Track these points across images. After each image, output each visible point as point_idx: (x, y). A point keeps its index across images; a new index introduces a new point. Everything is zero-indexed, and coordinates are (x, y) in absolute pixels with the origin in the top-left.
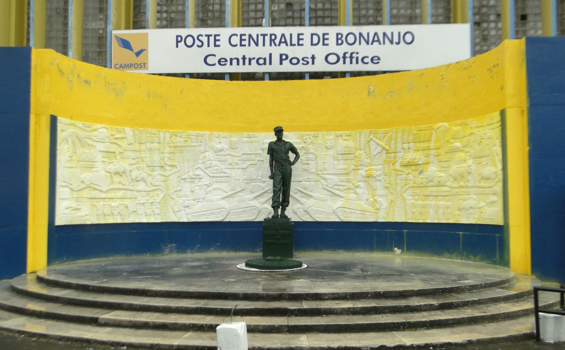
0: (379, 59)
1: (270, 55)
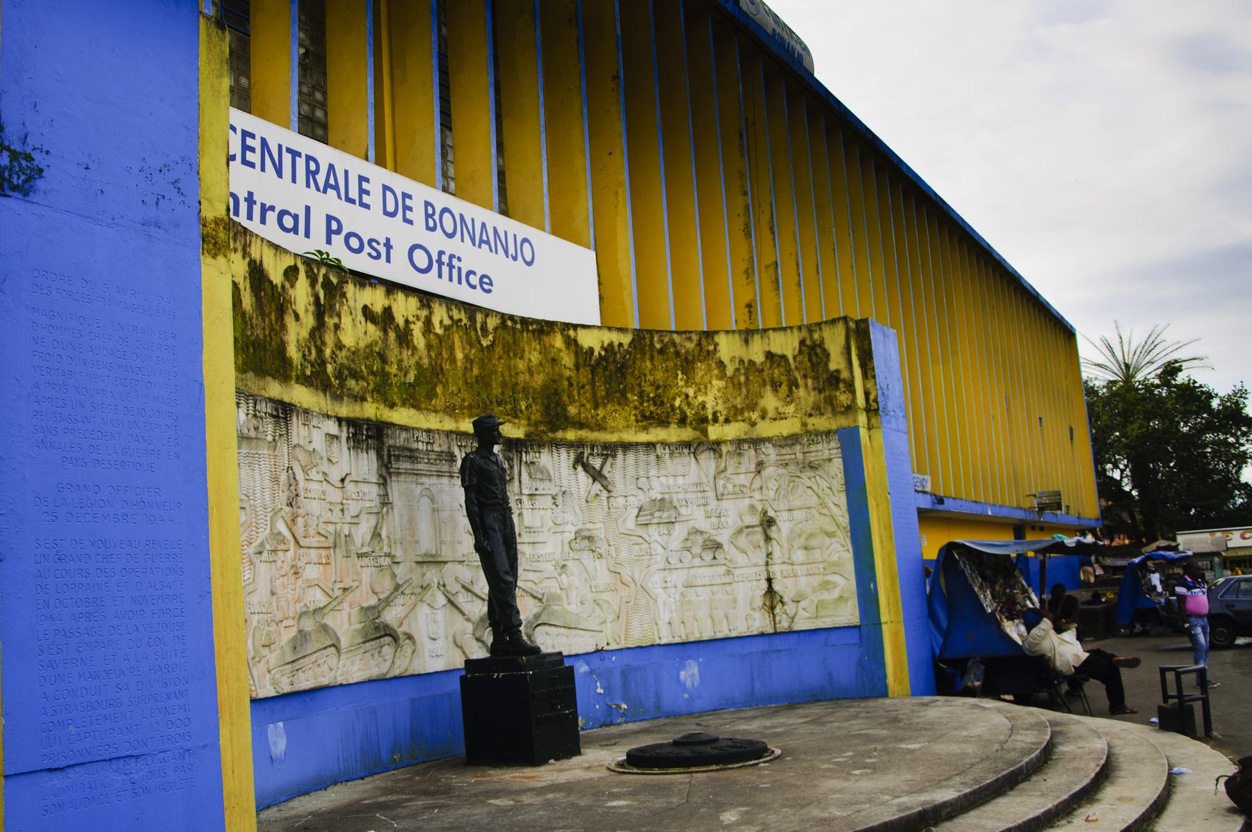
0: (491, 284)
1: (308, 209)
